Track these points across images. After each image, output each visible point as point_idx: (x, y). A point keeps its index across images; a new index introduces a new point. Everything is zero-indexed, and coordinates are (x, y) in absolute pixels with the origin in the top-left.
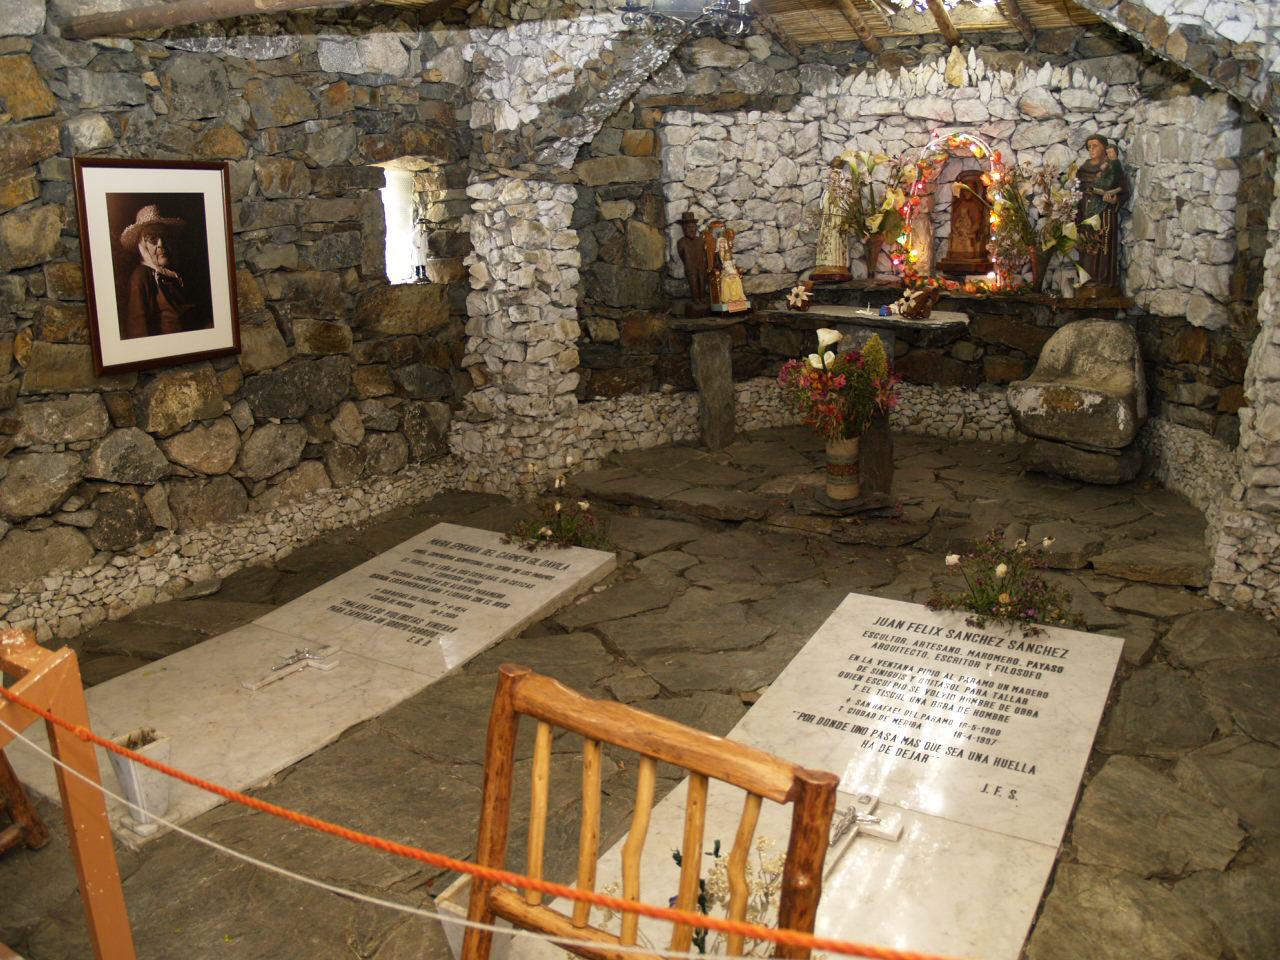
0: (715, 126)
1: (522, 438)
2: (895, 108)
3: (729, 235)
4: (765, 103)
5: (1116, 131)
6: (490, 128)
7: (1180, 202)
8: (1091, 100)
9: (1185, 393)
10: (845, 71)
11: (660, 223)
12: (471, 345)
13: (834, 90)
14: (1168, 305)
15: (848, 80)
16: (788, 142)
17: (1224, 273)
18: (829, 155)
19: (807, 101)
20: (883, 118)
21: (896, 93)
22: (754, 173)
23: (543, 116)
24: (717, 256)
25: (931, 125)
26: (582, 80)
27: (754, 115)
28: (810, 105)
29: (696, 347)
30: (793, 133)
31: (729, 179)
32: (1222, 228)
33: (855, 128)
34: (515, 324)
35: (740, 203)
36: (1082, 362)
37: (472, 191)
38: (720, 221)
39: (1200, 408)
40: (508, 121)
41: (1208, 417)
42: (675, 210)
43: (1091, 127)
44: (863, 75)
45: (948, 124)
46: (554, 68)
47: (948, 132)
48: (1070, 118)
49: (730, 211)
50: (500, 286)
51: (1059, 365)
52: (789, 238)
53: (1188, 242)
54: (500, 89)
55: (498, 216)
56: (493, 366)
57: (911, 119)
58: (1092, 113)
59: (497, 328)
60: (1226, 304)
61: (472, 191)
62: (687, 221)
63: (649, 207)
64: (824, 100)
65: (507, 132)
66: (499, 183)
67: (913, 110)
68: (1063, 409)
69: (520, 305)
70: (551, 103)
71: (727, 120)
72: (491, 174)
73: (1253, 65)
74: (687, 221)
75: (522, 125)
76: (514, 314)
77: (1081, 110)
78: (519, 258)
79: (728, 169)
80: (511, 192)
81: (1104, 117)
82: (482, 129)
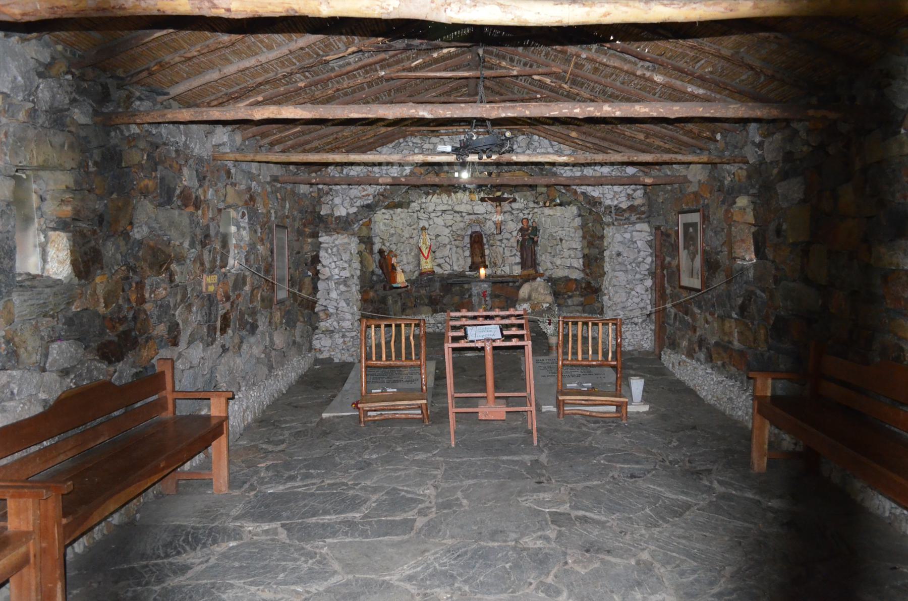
0: (388, 213)
1: (352, 337)
2: (450, 208)
3: (396, 256)
4: (400, 205)
5: (530, 217)
6: (332, 215)
7: (561, 240)
8: (521, 206)
9: (569, 302)
10: (427, 194)
11: (371, 252)
12: (320, 303)
13: (424, 200)
14: (560, 273)
15: (430, 197)
16: (409, 220)
17: (581, 261)
18: (421, 225)
19: (413, 204)
20: (444, 211)
21: (450, 202)
22: (400, 232)
23: (358, 211)
24: (393, 265)
25: (464, 214)
26: (377, 199)
27: (399, 210)
28: (415, 206)
29: (390, 302)
30: (411, 216)
31: (392, 235)
32: (579, 247)
33: (433, 215)
34: (342, 292)
35: (396, 244)
36: (534, 295)
37: (320, 239)
38: (391, 251)
39: (577, 305)
40: (341, 212)
41: (580, 308)
42: (376, 248)
43: (521, 215)
44: (436, 196)
45: (469, 214)
46: (364, 193)
47: (471, 217)
48: (514, 212)
49: (394, 247)
50: (337, 277)
51: (527, 297)
52: (411, 259)
53: (566, 253)
54: (337, 201)
55: (335, 250)
56: (331, 310)
57: (455, 212)
58: (521, 210)
59: (334, 295)
60: (583, 271)
61: (320, 239)
62: (381, 252)
63: (369, 246)
64: (420, 204)
65: (339, 218)
66: (334, 237)
67: (457, 208)
68: (536, 310)
69: (345, 285)
70: (363, 206)
71: (392, 212)
72: (329, 231)
73: (600, 203)
74: (381, 252)
75: (348, 214)
76: (342, 288)
77: (518, 210)
78: (346, 265)
79: (392, 231)
80: (341, 239)
81: (526, 212)
82: (328, 215)
